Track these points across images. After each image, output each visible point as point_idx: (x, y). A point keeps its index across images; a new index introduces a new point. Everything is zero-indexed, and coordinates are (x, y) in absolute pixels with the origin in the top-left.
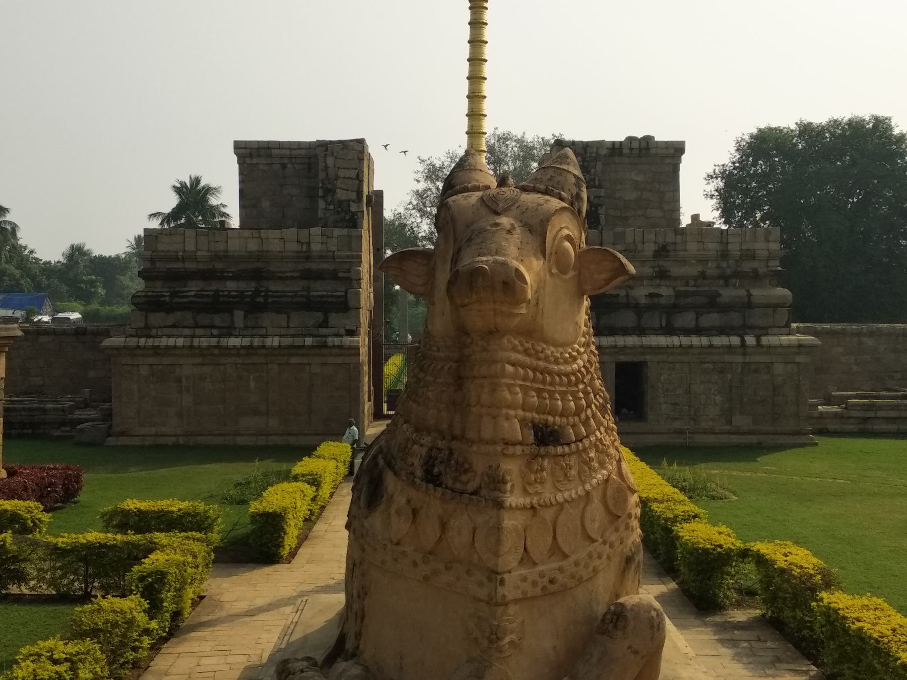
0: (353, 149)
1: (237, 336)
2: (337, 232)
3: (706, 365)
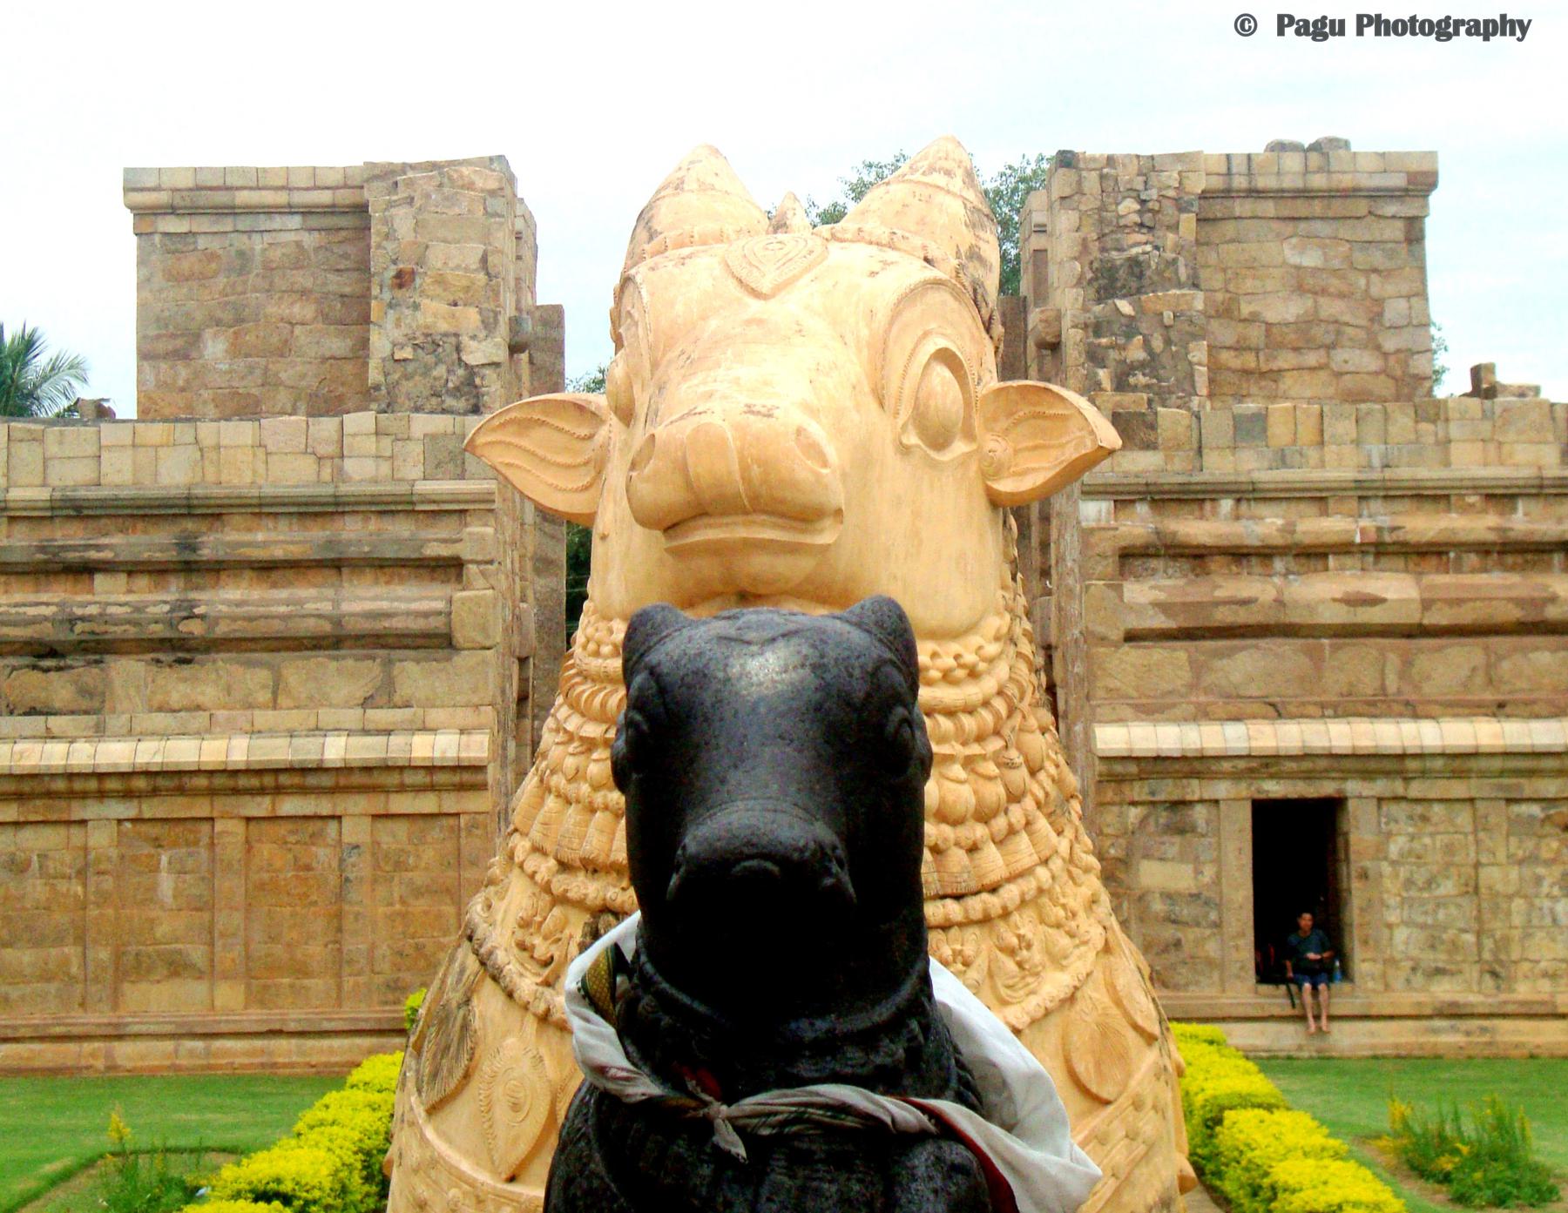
0: (470, 186)
1: (119, 737)
2: (424, 424)
3: (1524, 809)
